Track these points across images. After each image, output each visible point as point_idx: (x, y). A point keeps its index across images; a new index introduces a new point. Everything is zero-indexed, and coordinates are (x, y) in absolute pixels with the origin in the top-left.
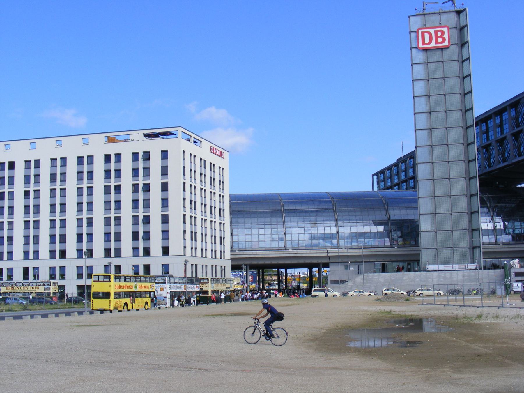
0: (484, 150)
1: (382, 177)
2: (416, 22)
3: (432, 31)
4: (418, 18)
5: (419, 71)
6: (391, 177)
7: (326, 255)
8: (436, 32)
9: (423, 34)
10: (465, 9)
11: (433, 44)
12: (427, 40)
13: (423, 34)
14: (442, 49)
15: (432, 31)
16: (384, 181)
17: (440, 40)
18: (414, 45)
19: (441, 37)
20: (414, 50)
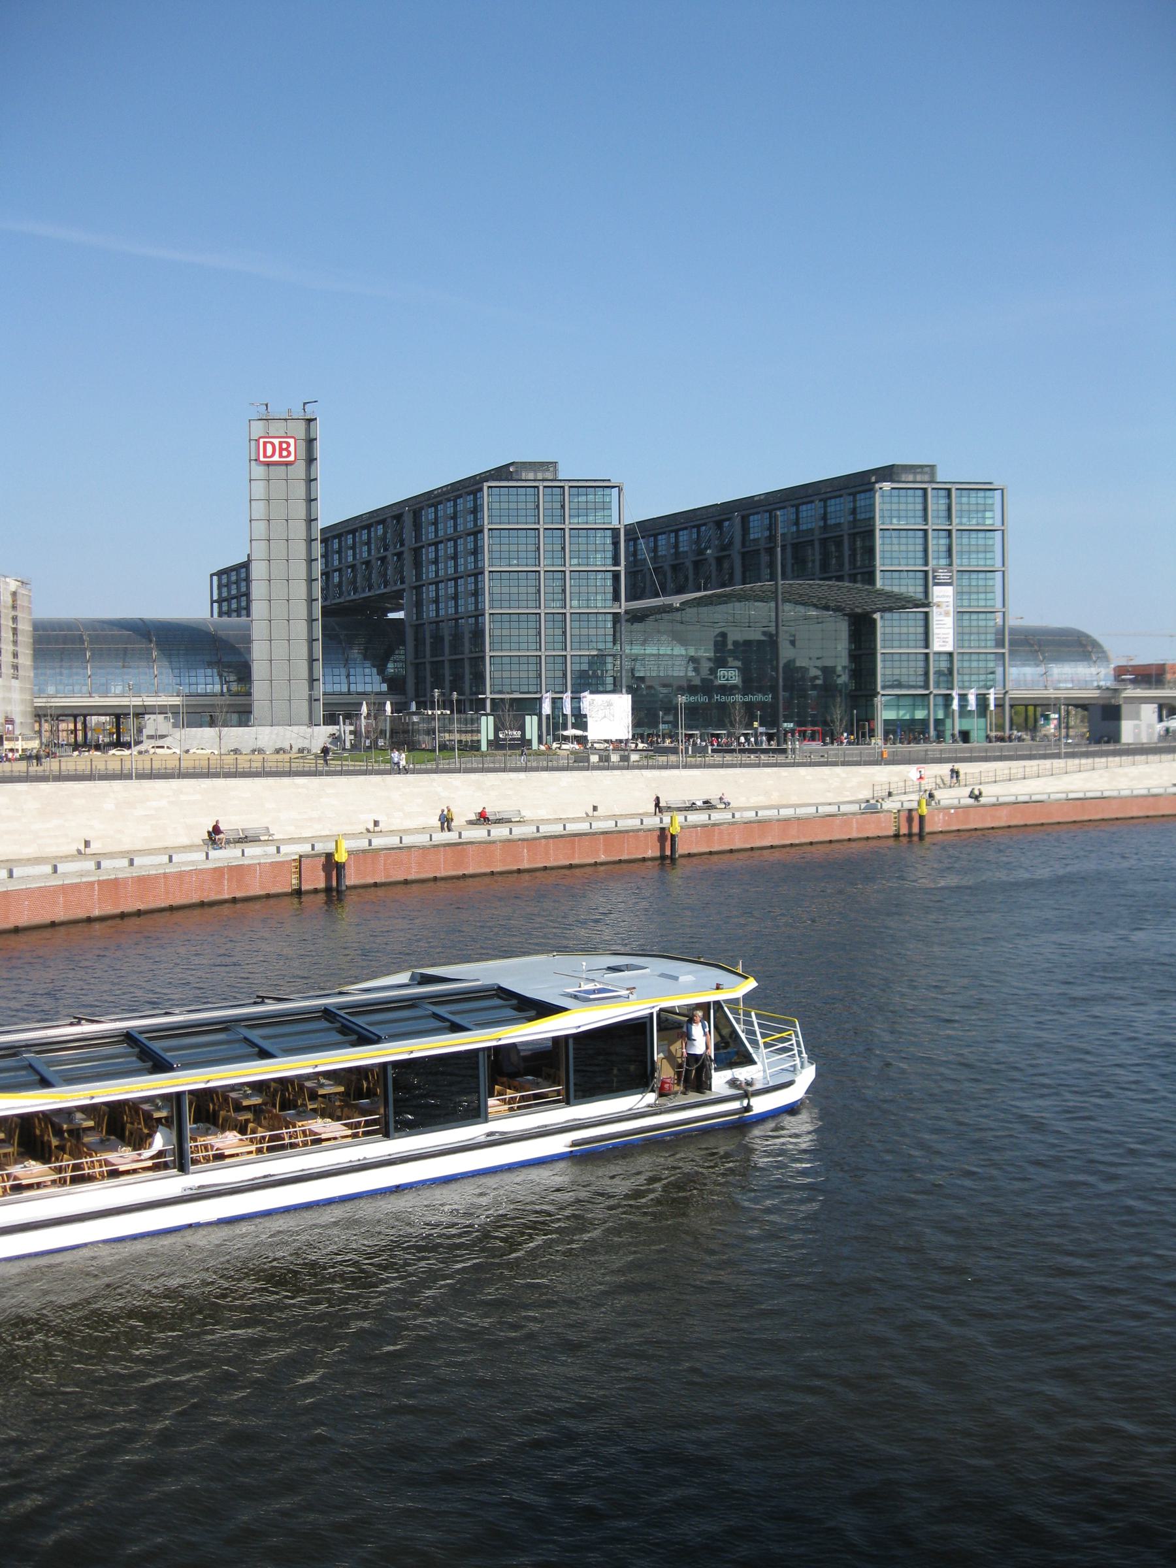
0: (349, 570)
1: (224, 581)
2: (258, 429)
3: (276, 441)
5: (259, 489)
6: (237, 583)
7: (141, 703)
8: (281, 443)
10: (316, 419)
11: (276, 458)
12: (269, 453)
13: (265, 443)
14: (287, 464)
15: (276, 441)
16: (228, 585)
17: (285, 453)
19: (286, 449)
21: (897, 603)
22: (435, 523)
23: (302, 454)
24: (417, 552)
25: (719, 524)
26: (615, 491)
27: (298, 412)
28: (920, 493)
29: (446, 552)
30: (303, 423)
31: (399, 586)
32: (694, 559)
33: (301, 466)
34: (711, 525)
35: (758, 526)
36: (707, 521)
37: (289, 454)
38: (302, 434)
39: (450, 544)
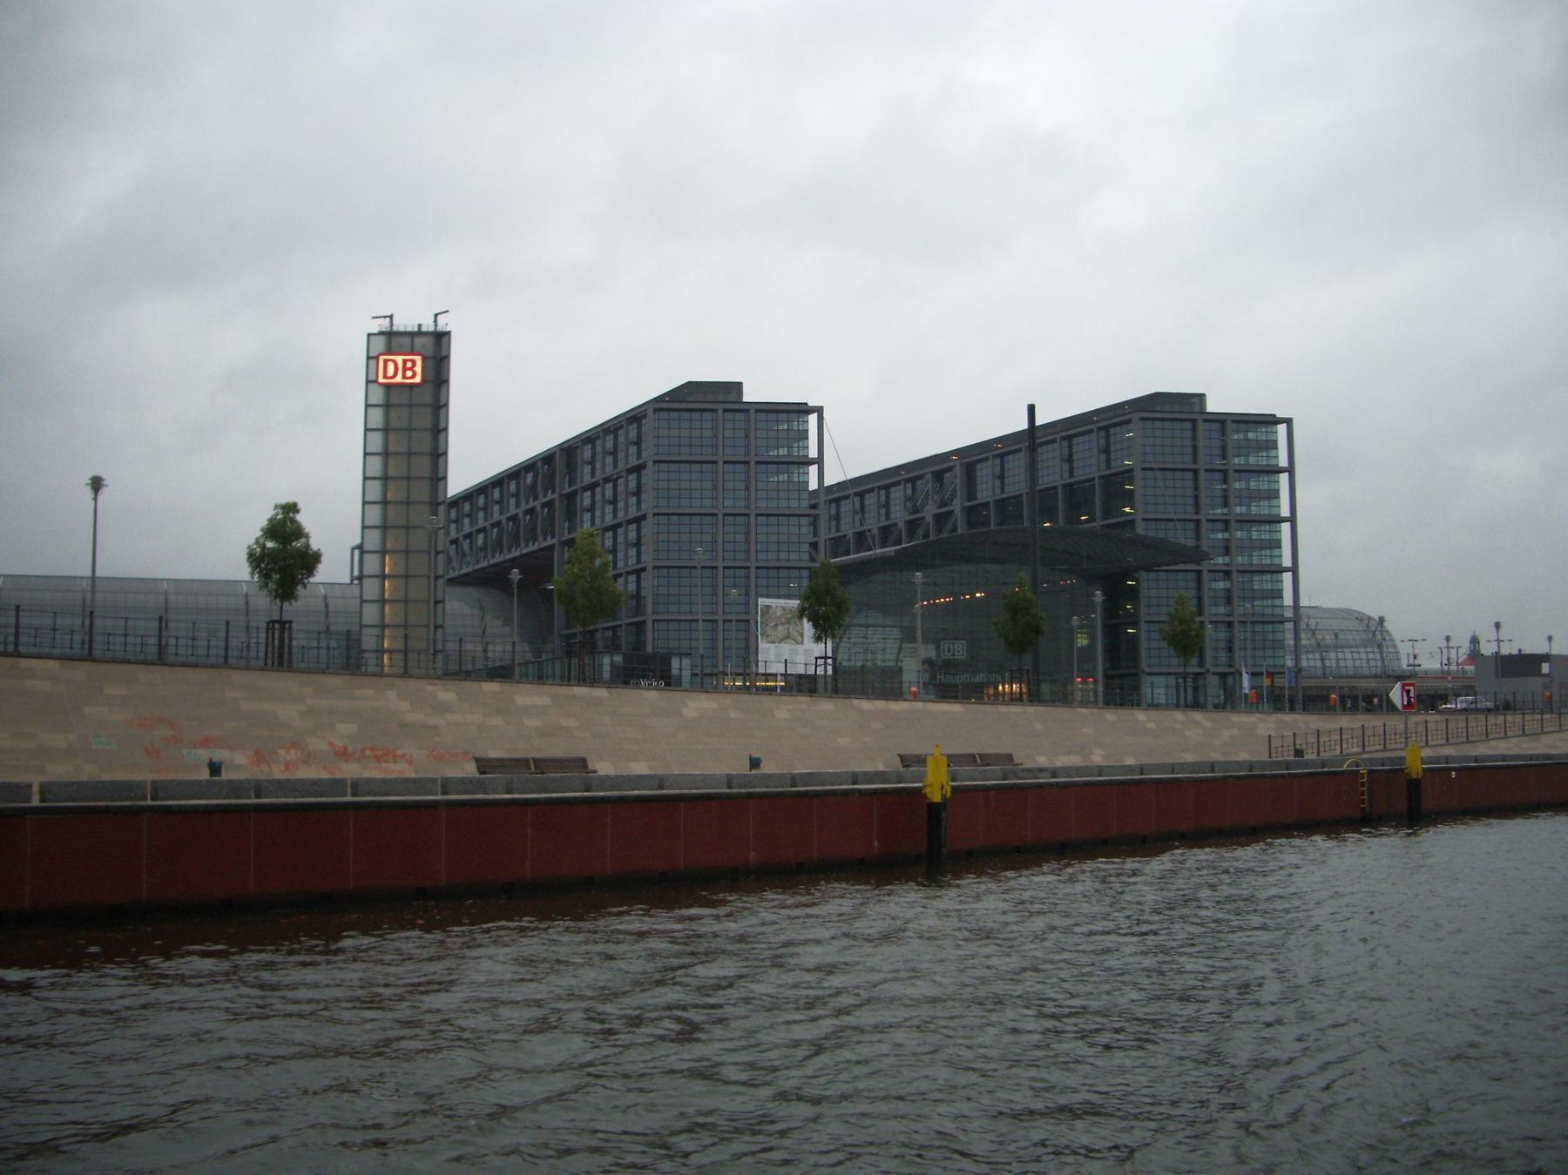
3: (399, 359)
8: (405, 362)
9: (386, 362)
11: (399, 379)
12: (391, 372)
13: (386, 362)
14: (412, 386)
18: (372, 377)
19: (411, 369)
20: (371, 386)
21: (1165, 555)
22: (592, 462)
24: (570, 498)
25: (939, 476)
26: (813, 418)
27: (428, 326)
28: (1188, 425)
29: (603, 495)
31: (550, 542)
32: (908, 518)
33: (429, 387)
34: (929, 476)
35: (984, 473)
37: (414, 376)
38: (430, 352)
39: (609, 486)
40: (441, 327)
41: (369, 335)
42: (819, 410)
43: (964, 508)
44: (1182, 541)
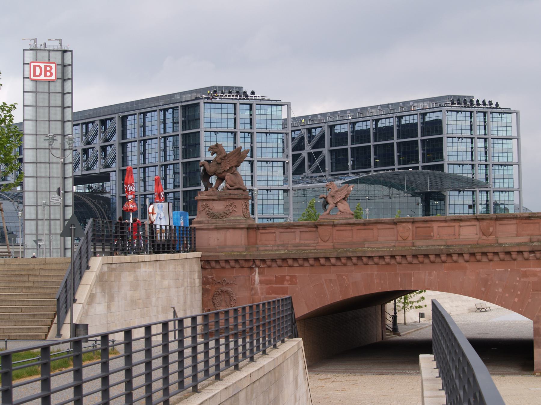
3: (43, 65)
4: (31, 52)
8: (46, 67)
11: (42, 77)
12: (38, 73)
13: (35, 66)
14: (49, 81)
17: (48, 74)
19: (49, 71)
23: (60, 76)
26: (285, 108)
30: (59, 54)
33: (60, 82)
34: (305, 131)
36: (300, 128)
38: (59, 62)
40: (63, 49)
41: (24, 50)
42: (288, 105)
43: (329, 150)
44: (465, 175)
